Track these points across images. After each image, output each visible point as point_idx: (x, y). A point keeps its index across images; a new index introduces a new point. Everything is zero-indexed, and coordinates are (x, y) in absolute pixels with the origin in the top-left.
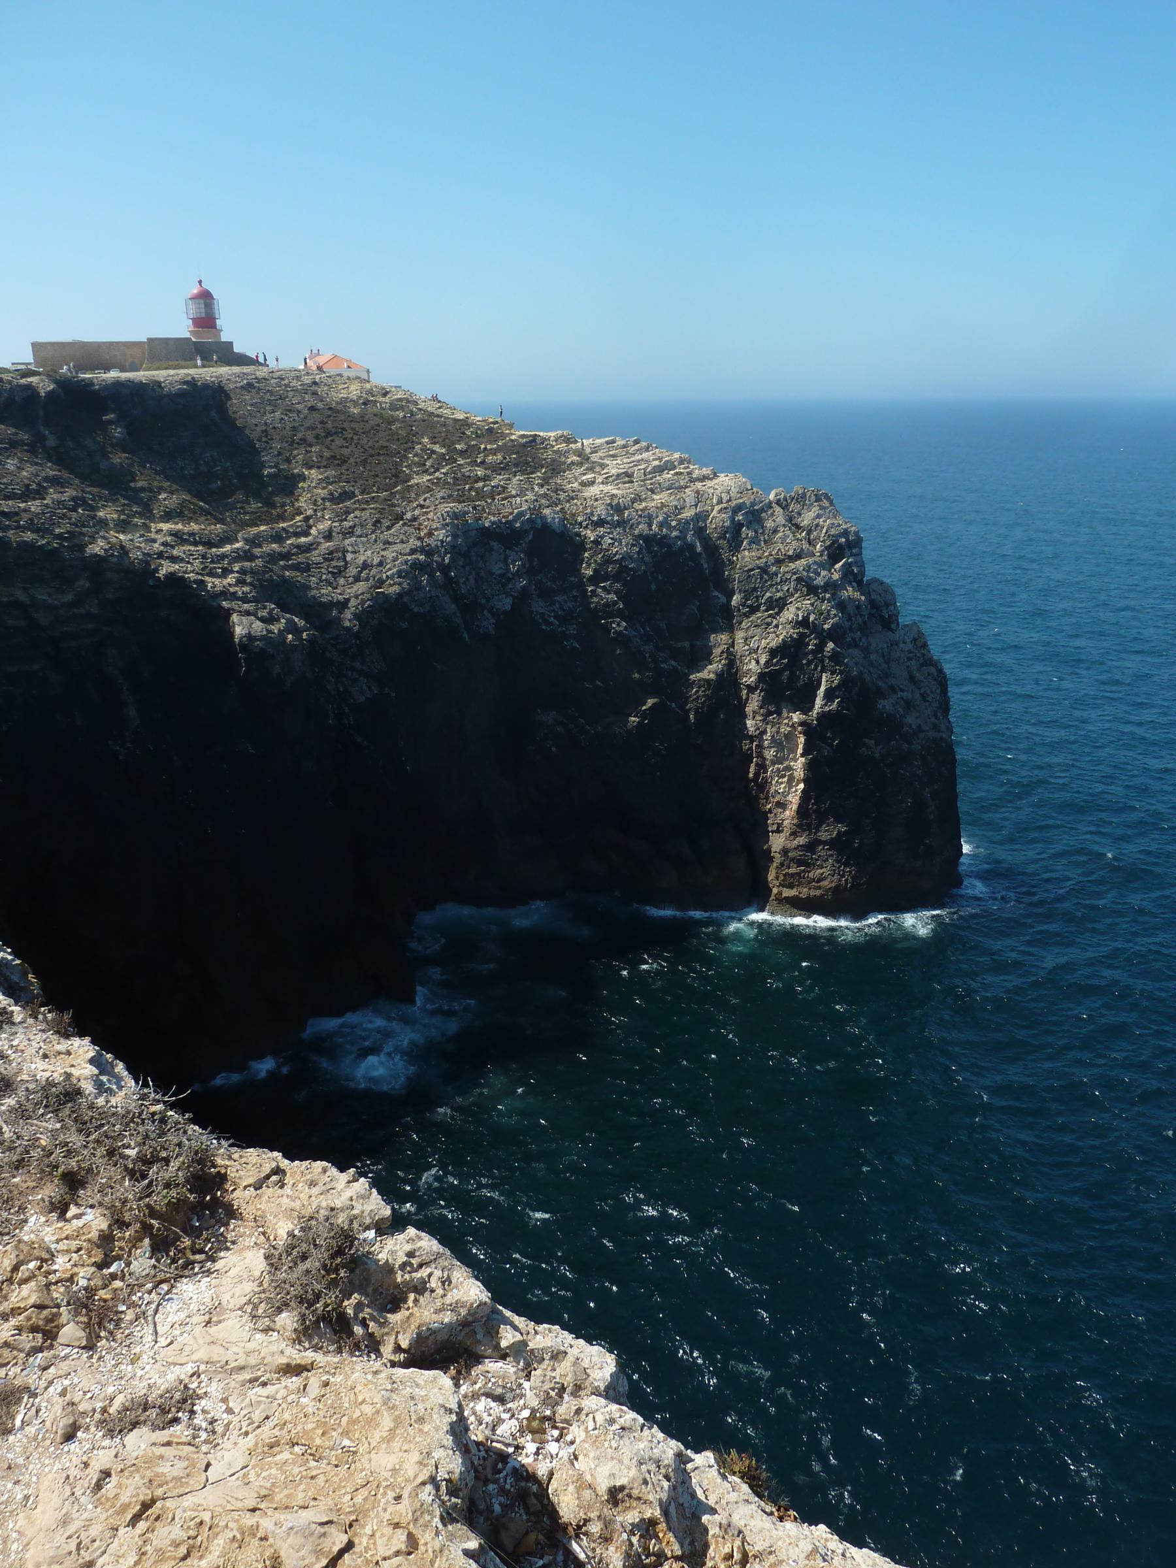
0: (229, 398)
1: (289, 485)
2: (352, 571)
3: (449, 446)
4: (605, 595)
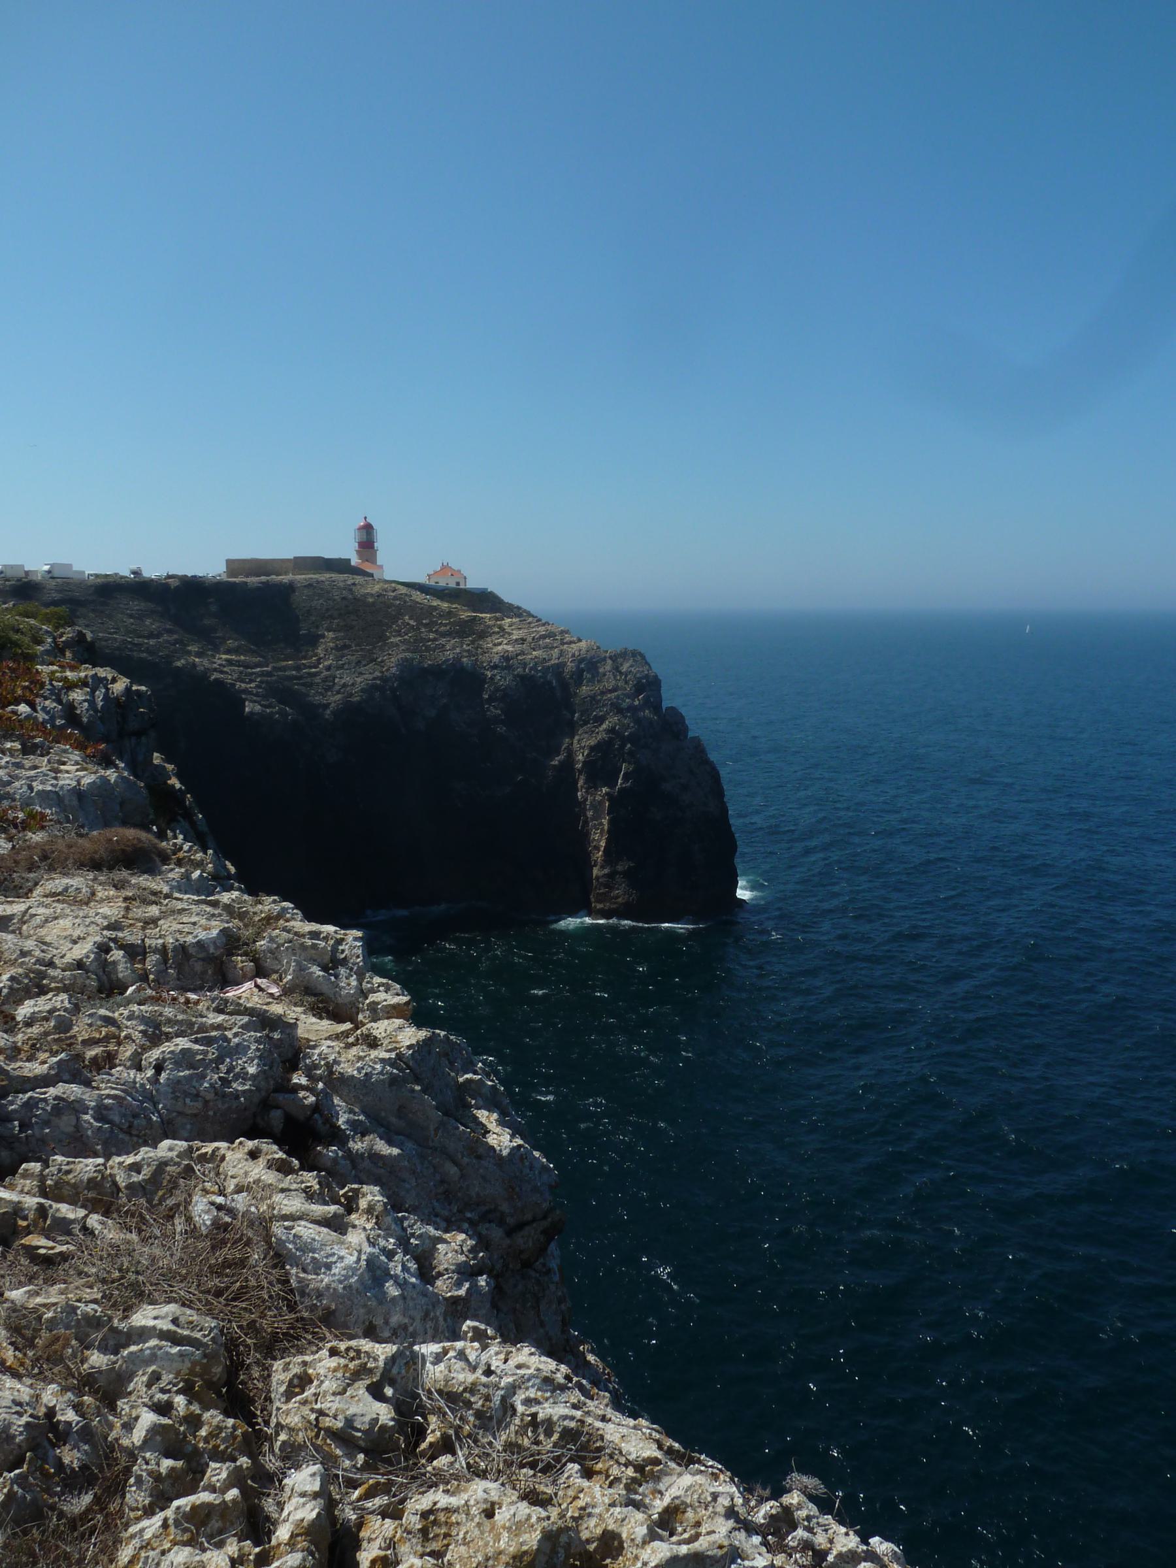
0: (294, 591)
1: (314, 640)
2: (337, 688)
3: (419, 620)
4: (494, 711)
